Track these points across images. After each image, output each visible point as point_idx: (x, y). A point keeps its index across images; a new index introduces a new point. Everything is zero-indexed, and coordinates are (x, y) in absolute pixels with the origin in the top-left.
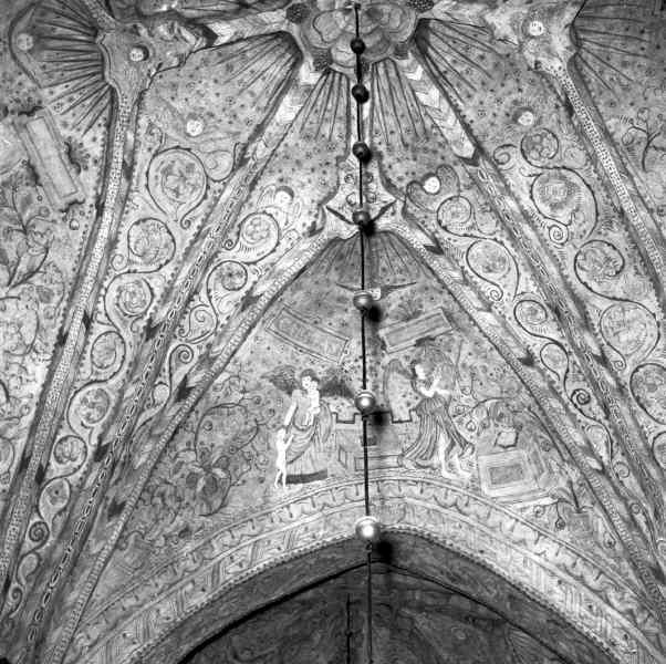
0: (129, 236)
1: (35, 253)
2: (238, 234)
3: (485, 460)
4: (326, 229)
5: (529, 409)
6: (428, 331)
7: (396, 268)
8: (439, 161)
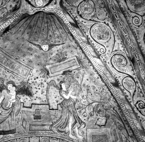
3: (90, 131)
4: (22, 8)
5: (114, 109)
6: (69, 68)
7: (56, 36)
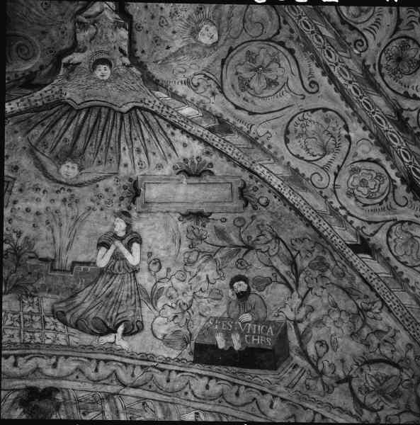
0: (297, 156)
1: (276, 251)
2: (352, 28)
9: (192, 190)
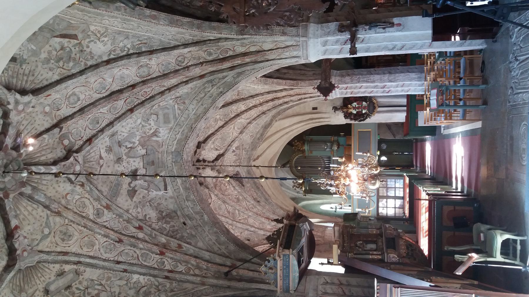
8: (58, 140)
9: (63, 280)
